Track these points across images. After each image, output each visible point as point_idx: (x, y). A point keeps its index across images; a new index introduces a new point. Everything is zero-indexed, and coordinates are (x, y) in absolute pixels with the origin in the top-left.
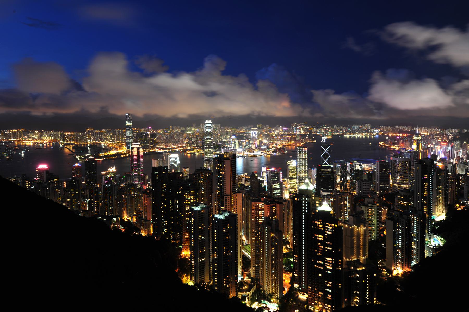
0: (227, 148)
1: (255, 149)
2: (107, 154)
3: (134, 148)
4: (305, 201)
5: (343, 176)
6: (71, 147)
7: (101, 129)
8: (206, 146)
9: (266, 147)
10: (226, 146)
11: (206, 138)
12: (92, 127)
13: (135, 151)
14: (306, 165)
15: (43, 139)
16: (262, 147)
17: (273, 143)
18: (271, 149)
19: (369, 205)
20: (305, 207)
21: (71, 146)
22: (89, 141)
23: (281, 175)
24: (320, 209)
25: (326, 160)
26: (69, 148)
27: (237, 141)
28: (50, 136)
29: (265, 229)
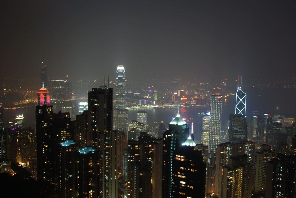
0: (146, 99)
1: (175, 101)
4: (174, 137)
5: (260, 130)
8: (117, 94)
9: (186, 99)
11: (118, 85)
14: (219, 115)
16: (182, 99)
17: (195, 95)
18: (192, 100)
19: (264, 153)
20: (173, 144)
23: (192, 126)
24: (183, 144)
25: (240, 111)
27: (156, 91)
29: (134, 168)
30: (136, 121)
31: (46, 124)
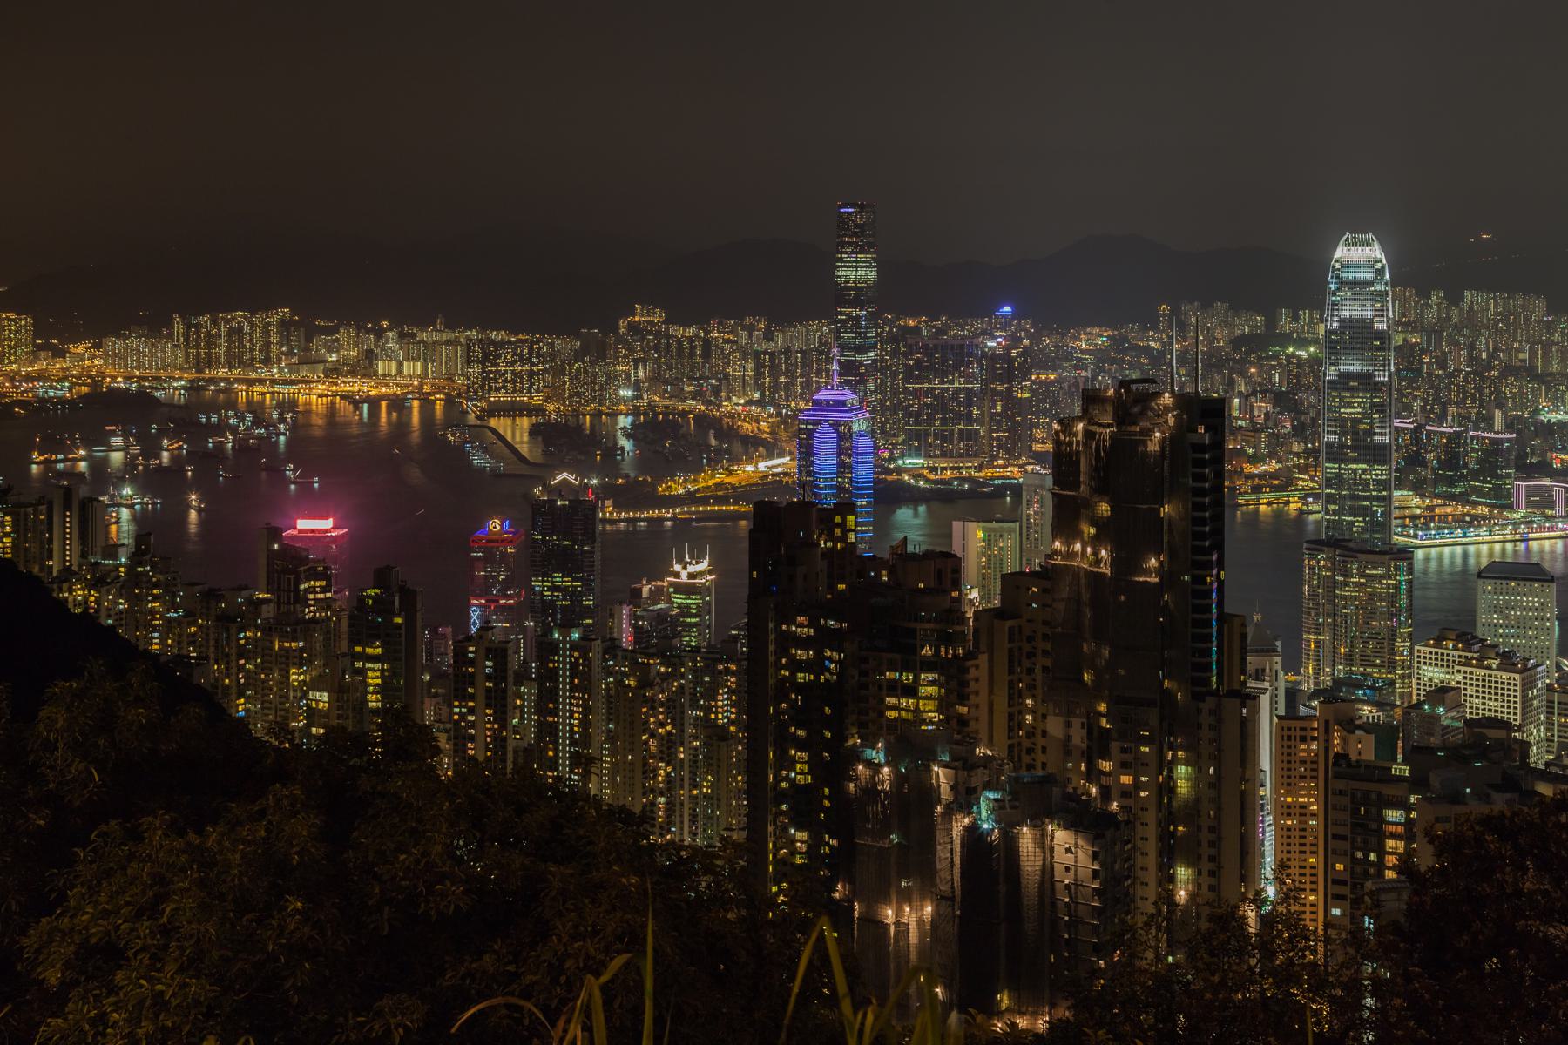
2: (711, 483)
3: (816, 423)
6: (518, 431)
7: (702, 321)
10: (1557, 465)
12: (650, 301)
13: (826, 441)
15: (380, 372)
21: (525, 423)
22: (626, 393)
26: (509, 438)
28: (416, 359)
30: (1467, 638)
31: (801, 619)
